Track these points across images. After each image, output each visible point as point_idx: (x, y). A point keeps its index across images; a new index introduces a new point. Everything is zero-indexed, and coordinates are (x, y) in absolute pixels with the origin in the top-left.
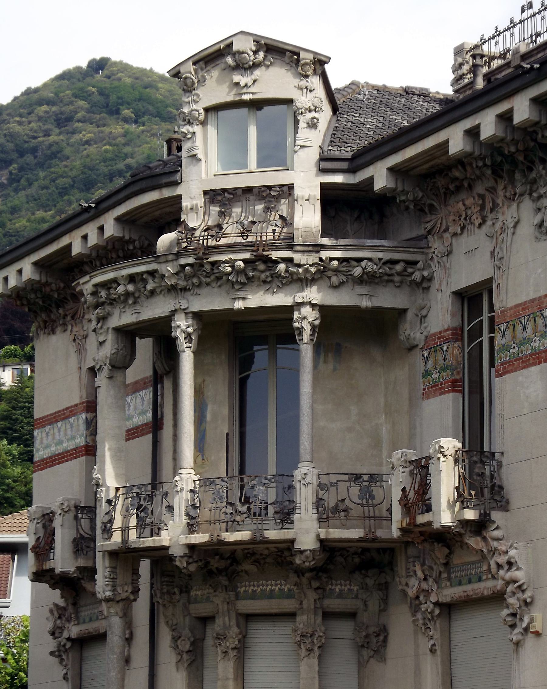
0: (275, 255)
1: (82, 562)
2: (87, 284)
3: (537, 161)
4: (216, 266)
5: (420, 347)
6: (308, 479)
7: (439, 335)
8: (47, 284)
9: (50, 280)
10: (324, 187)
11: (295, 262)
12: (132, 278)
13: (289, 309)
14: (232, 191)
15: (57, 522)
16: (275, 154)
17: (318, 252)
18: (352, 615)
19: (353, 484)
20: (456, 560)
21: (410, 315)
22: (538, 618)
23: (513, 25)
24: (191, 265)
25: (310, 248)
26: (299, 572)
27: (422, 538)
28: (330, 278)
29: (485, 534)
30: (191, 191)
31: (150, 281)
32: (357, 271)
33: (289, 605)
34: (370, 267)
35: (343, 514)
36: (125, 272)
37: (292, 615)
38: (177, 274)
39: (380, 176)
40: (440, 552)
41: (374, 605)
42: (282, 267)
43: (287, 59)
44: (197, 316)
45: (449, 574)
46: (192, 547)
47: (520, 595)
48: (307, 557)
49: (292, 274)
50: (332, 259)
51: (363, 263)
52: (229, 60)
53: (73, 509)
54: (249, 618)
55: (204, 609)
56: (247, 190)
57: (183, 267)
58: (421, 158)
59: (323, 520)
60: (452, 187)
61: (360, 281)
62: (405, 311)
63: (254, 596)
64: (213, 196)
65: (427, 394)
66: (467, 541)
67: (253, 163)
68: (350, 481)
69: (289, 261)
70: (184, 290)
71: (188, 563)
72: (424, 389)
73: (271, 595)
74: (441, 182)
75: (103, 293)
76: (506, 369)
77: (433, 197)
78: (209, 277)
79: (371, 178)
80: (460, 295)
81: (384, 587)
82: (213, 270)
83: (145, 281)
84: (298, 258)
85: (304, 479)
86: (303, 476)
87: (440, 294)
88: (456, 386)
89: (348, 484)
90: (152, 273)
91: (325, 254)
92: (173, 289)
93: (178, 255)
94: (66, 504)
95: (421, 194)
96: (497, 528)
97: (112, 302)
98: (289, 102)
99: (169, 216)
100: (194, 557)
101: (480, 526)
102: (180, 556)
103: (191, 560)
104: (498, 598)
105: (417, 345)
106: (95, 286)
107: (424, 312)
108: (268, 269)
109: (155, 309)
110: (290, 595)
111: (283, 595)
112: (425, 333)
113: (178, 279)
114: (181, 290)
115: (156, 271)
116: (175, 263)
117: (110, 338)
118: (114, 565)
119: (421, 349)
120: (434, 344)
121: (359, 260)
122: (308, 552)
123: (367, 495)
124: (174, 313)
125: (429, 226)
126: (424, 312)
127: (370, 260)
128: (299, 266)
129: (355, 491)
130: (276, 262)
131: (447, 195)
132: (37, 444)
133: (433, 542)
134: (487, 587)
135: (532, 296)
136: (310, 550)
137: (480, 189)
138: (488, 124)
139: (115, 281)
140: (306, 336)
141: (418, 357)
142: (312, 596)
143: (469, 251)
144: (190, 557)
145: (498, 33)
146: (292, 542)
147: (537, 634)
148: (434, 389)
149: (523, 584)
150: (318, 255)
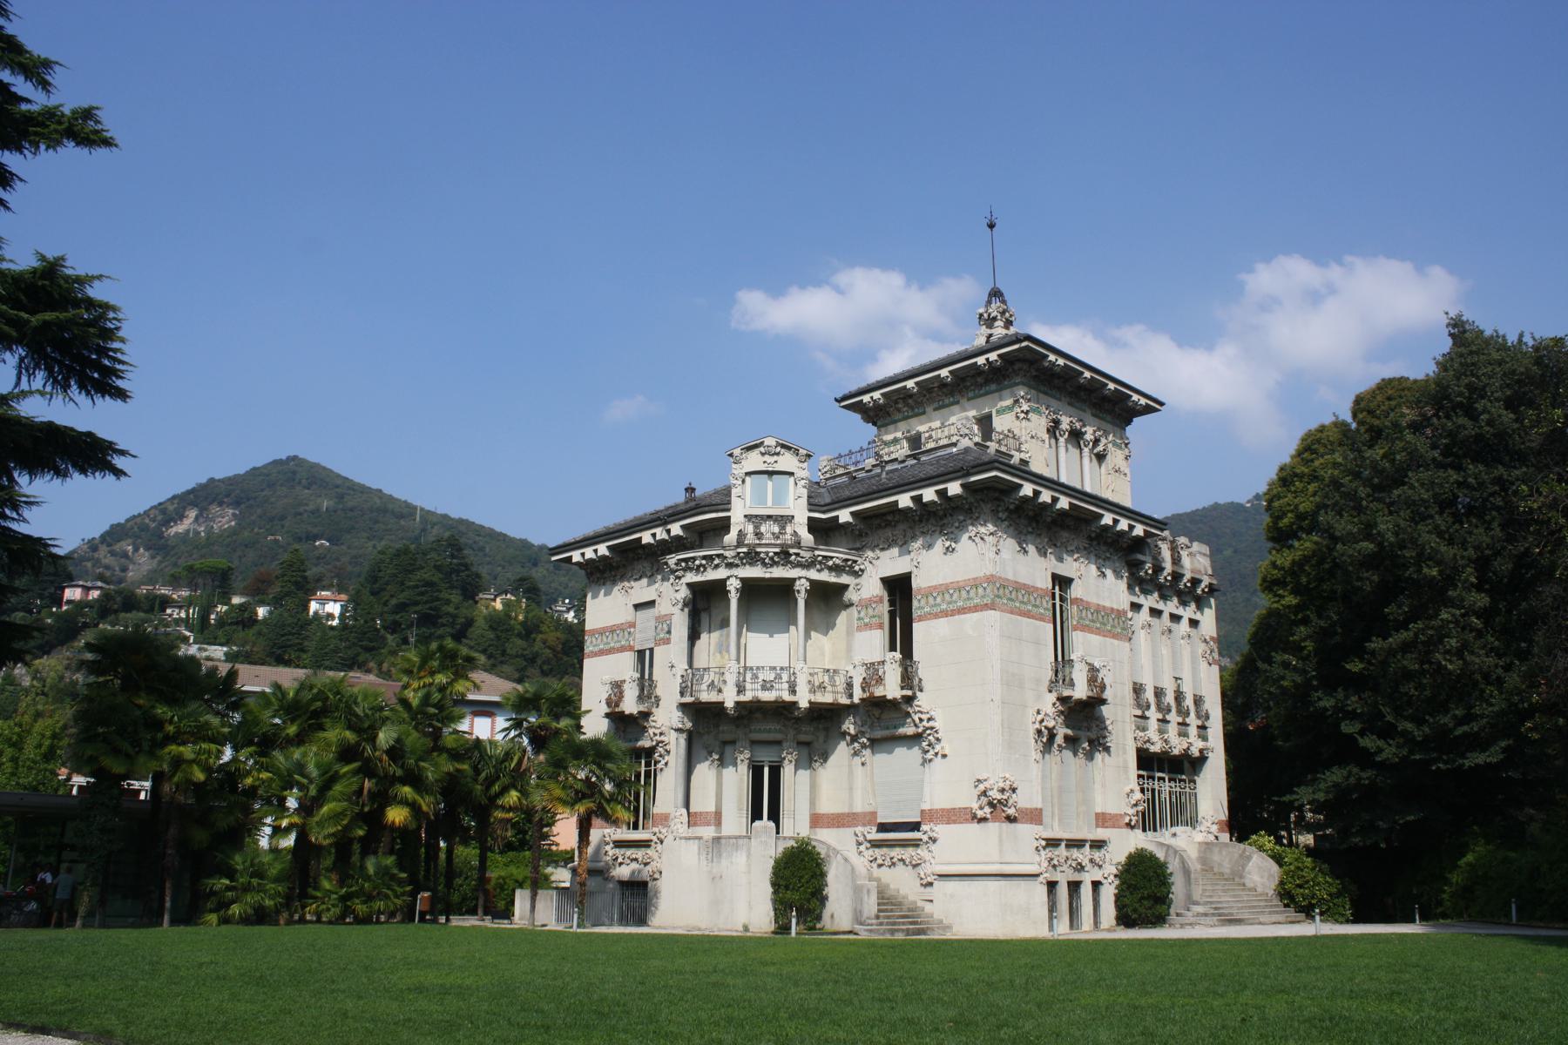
0: (792, 551)
1: (642, 708)
2: (672, 560)
7: (870, 600)
10: (810, 519)
12: (704, 557)
14: (762, 517)
15: (626, 687)
16: (779, 498)
18: (808, 744)
20: (885, 716)
22: (945, 746)
23: (862, 450)
26: (798, 719)
30: (737, 514)
33: (779, 736)
37: (779, 743)
39: (844, 516)
40: (877, 712)
41: (821, 740)
44: (742, 580)
46: (737, 703)
54: (753, 743)
55: (728, 737)
56: (769, 517)
59: (813, 691)
61: (830, 569)
62: (846, 587)
63: (760, 731)
64: (748, 517)
65: (859, 629)
67: (770, 503)
73: (769, 731)
74: (877, 521)
76: (921, 619)
80: (882, 579)
81: (827, 729)
84: (803, 553)
88: (881, 626)
90: (718, 556)
92: (730, 566)
93: (737, 547)
97: (685, 570)
98: (792, 474)
99: (724, 525)
101: (909, 700)
104: (918, 737)
109: (712, 575)
110: (780, 731)
111: (776, 731)
117: (684, 588)
120: (867, 604)
123: (832, 679)
129: (826, 678)
131: (879, 527)
132: (587, 644)
134: (909, 730)
137: (901, 527)
138: (929, 494)
139: (694, 559)
141: (853, 610)
142: (792, 733)
145: (851, 453)
146: (795, 703)
147: (944, 756)
148: (868, 626)
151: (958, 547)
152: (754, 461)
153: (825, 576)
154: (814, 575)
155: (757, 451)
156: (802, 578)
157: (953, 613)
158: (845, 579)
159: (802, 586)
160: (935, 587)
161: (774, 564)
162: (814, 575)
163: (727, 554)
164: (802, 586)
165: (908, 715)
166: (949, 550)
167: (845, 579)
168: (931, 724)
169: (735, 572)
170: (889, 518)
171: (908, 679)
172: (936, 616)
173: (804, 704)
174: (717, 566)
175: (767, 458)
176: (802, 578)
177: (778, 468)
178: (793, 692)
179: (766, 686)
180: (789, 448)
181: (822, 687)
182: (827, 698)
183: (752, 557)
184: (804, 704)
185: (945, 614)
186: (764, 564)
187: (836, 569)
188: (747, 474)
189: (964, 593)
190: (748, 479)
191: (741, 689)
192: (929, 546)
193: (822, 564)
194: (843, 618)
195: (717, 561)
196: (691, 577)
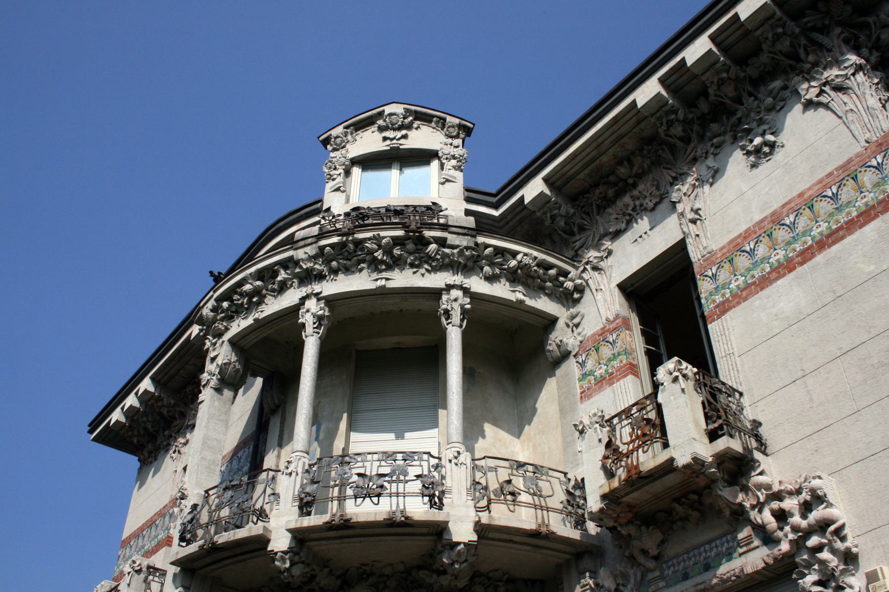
0: (428, 234)
3: (745, 95)
4: (360, 247)
5: (573, 353)
6: (462, 459)
8: (159, 399)
9: (162, 395)
11: (449, 242)
12: (260, 275)
13: (435, 294)
17: (475, 237)
19: (515, 472)
20: (671, 550)
21: (561, 324)
24: (332, 246)
25: (465, 231)
27: (630, 515)
28: (482, 269)
29: (745, 482)
31: (282, 272)
32: (513, 263)
34: (527, 260)
35: (509, 497)
36: (253, 269)
38: (314, 258)
40: (650, 541)
42: (433, 247)
43: (433, 124)
44: (331, 301)
45: (662, 571)
47: (839, 545)
48: (459, 553)
49: (445, 256)
50: (487, 246)
51: (519, 257)
52: (380, 122)
53: (144, 569)
57: (321, 249)
58: (584, 154)
60: (611, 192)
62: (554, 320)
66: (720, 493)
68: (511, 468)
69: (442, 242)
70: (320, 277)
71: (292, 565)
72: (582, 393)
75: (225, 304)
76: (724, 308)
77: (585, 216)
78: (350, 260)
79: (522, 198)
82: (355, 251)
83: (276, 274)
84: (452, 239)
85: (456, 458)
86: (456, 454)
87: (600, 293)
89: (510, 471)
90: (285, 264)
91: (481, 239)
92: (308, 277)
94: (138, 563)
95: (572, 211)
96: (761, 473)
100: (301, 555)
102: (282, 552)
103: (297, 558)
105: (570, 352)
106: (217, 300)
107: (576, 321)
108: (417, 251)
112: (580, 338)
113: (315, 263)
114: (316, 276)
115: (291, 259)
116: (314, 245)
118: (187, 585)
119: (575, 356)
121: (514, 254)
122: (462, 546)
124: (303, 300)
125: (578, 244)
126: (576, 321)
127: (526, 255)
128: (453, 247)
130: (430, 243)
131: (607, 202)
133: (640, 526)
135: (757, 217)
136: (465, 544)
140: (456, 317)
141: (571, 367)
143: (641, 237)
144: (296, 554)
149: (843, 526)
150: (473, 239)
151: (782, 139)
152: (370, 142)
153: (502, 290)
154: (478, 285)
155: (374, 128)
156: (457, 291)
157: (806, 255)
158: (544, 304)
159: (454, 304)
160: (746, 235)
161: (396, 263)
162: (478, 285)
163: (300, 254)
164: (454, 304)
165: (739, 516)
166: (759, 155)
167: (544, 304)
168: (815, 515)
169: (317, 288)
170: (623, 171)
171: (719, 413)
172: (764, 282)
173: (462, 532)
174: (283, 287)
175: (389, 134)
176: (457, 291)
177: (408, 144)
178: (436, 502)
179: (370, 490)
180: (426, 119)
181: (508, 493)
182: (524, 518)
183: (348, 256)
184: (462, 532)
185: (787, 267)
186: (375, 265)
187: (519, 276)
188: (355, 162)
189: (824, 207)
190: (356, 171)
191: (305, 506)
192: (716, 174)
193: (498, 265)
194: (549, 396)
195: (282, 275)
196: (239, 325)
